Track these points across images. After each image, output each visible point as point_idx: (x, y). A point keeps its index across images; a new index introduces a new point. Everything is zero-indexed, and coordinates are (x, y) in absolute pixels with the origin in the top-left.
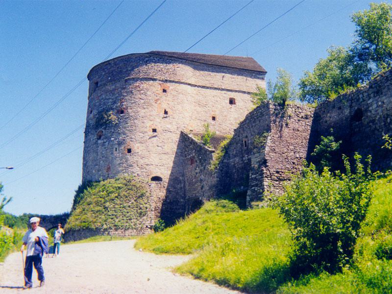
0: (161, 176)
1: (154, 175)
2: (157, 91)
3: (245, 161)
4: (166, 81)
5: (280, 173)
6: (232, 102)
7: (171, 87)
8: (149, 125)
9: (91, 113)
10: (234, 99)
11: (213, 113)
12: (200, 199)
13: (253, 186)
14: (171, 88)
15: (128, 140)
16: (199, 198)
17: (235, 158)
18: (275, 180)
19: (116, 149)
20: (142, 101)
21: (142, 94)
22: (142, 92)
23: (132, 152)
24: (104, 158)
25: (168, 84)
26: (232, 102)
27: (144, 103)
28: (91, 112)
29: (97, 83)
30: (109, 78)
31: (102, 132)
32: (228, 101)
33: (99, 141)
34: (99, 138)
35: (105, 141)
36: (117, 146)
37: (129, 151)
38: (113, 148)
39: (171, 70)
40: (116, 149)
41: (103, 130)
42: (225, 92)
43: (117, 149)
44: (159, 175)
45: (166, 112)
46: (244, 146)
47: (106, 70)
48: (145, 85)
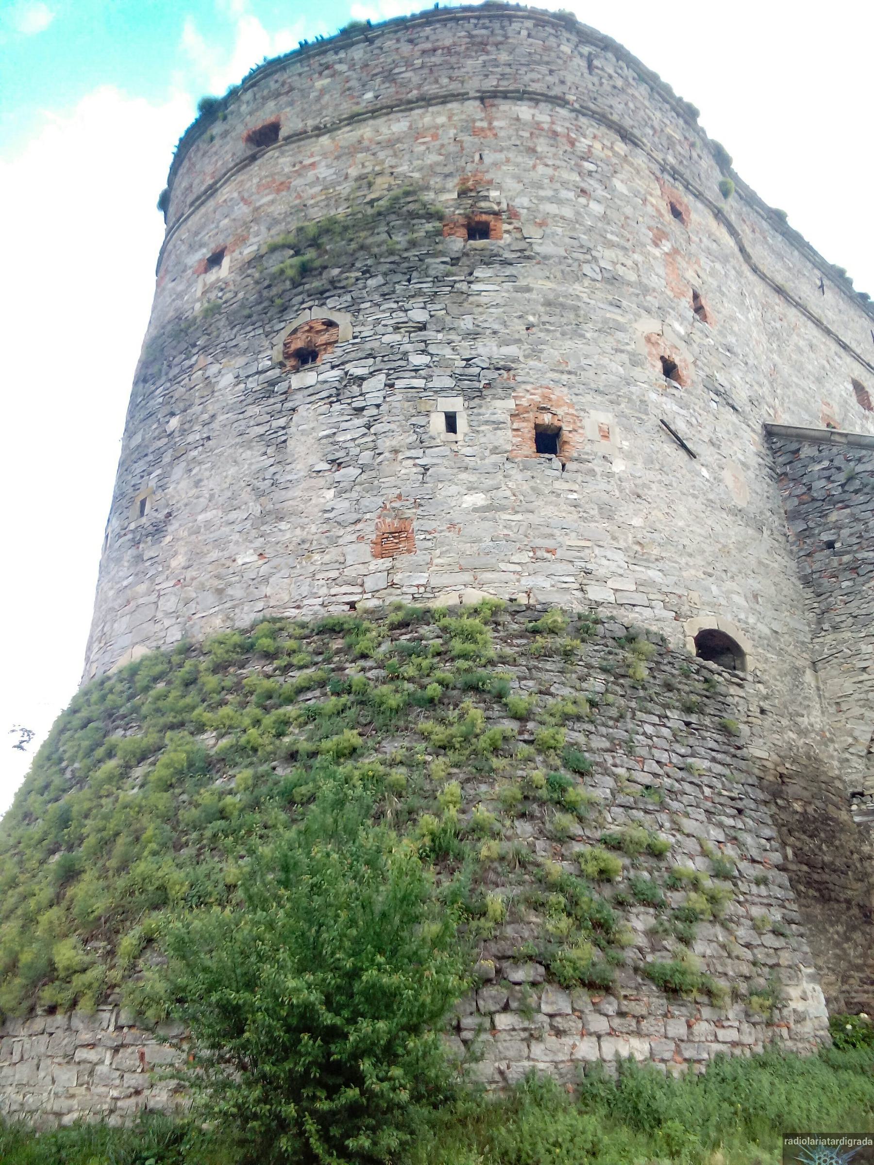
1: (709, 623)
15: (529, 370)
21: (590, 173)
24: (352, 472)
30: (369, 95)
31: (330, 324)
34: (306, 357)
35: (359, 372)
36: (456, 404)
37: (548, 441)
38: (428, 414)
41: (343, 320)
43: (461, 423)
47: (342, 67)
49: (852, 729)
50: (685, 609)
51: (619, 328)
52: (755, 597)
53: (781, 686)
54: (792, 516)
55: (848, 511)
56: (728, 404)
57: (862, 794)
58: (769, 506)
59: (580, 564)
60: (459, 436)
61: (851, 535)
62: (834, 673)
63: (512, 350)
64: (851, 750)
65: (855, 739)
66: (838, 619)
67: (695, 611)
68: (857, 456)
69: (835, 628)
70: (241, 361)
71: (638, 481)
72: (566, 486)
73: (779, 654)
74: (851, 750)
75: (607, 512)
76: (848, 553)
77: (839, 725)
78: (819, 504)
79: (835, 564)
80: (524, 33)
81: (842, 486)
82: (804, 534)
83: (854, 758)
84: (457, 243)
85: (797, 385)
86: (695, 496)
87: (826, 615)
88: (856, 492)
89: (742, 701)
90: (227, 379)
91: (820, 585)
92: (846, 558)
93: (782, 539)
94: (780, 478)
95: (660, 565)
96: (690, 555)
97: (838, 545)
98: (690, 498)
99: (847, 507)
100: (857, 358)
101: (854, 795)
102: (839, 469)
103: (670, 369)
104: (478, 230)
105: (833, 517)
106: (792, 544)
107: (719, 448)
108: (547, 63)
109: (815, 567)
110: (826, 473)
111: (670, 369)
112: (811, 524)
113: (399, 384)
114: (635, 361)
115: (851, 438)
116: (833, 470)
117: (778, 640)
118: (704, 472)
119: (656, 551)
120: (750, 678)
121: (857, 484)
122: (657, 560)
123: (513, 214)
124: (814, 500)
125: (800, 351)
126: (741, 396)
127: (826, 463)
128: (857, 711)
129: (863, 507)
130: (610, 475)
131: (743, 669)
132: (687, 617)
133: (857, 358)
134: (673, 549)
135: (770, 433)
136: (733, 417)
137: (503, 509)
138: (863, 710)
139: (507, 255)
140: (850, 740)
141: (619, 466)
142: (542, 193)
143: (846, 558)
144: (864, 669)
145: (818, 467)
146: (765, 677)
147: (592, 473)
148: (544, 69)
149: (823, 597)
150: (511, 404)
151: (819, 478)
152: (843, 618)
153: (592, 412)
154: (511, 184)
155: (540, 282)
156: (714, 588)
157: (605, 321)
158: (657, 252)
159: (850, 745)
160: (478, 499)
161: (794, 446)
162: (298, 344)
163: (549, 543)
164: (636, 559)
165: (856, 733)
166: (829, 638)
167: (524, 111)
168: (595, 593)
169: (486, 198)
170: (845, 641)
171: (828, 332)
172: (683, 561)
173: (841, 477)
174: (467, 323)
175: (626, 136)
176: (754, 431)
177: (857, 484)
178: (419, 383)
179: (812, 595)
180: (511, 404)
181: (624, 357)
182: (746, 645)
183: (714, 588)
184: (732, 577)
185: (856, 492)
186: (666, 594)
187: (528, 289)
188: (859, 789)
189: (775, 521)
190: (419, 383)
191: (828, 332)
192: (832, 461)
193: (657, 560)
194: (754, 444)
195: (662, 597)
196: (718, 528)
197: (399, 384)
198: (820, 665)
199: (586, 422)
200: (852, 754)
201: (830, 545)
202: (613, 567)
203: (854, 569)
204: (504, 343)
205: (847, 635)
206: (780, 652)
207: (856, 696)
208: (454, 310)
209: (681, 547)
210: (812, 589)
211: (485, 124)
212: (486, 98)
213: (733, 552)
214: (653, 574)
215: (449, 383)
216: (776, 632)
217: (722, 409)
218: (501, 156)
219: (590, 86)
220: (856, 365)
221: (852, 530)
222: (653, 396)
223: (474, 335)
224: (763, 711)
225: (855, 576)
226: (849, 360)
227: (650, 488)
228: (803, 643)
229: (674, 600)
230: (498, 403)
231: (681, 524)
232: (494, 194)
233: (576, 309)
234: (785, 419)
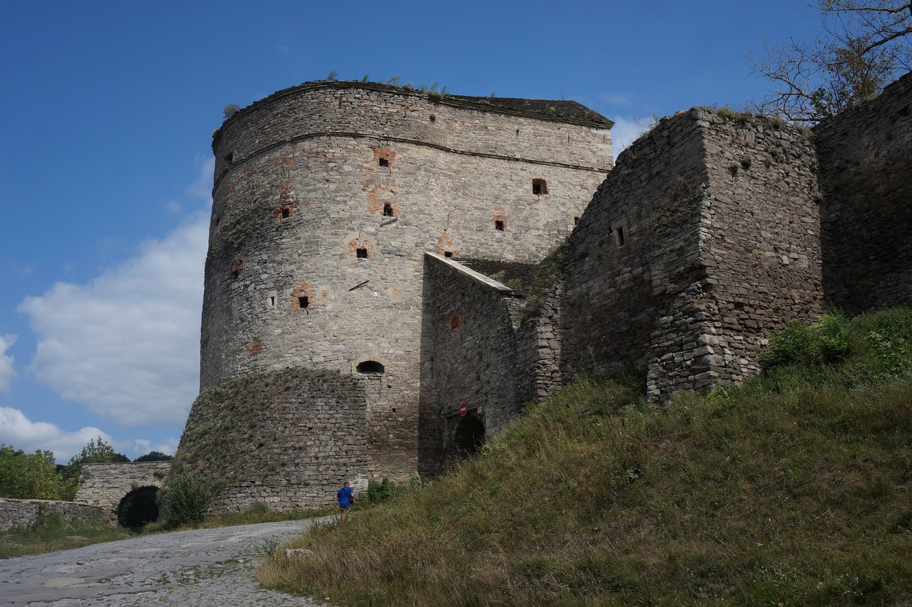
0: (383, 362)
1: (364, 358)
2: (367, 162)
3: (623, 287)
4: (387, 139)
5: (746, 308)
6: (539, 187)
7: (402, 154)
8: (350, 238)
9: (217, 225)
10: (543, 182)
11: (496, 213)
12: (479, 411)
13: (669, 349)
14: (398, 156)
16: (476, 410)
17: (591, 283)
18: (732, 329)
19: (273, 298)
20: (332, 186)
22: (331, 165)
23: (310, 306)
25: (393, 146)
26: (539, 187)
27: (337, 190)
28: (218, 221)
29: (229, 157)
31: (241, 261)
32: (529, 187)
33: (235, 285)
35: (248, 283)
36: (274, 293)
37: (304, 302)
39: (397, 117)
40: (273, 298)
42: (525, 165)
43: (276, 300)
44: (376, 357)
45: (388, 210)
46: (618, 243)
48: (337, 148)
51: (336, 244)
52: (397, 341)
59: (311, 349)
60: (275, 307)
63: (293, 267)
70: (221, 275)
72: (305, 321)
75: (322, 327)
80: (310, 97)
84: (279, 221)
90: (218, 283)
103: (362, 253)
104: (286, 213)
108: (319, 112)
111: (362, 253)
113: (258, 288)
114: (342, 257)
118: (376, 294)
119: (342, 338)
123: (297, 202)
130: (325, 312)
137: (287, 333)
139: (294, 224)
141: (329, 307)
142: (310, 188)
147: (318, 312)
148: (316, 117)
150: (291, 290)
153: (320, 287)
154: (298, 186)
155: (305, 234)
157: (330, 244)
158: (364, 194)
160: (279, 331)
162: (234, 270)
163: (301, 344)
164: (333, 342)
167: (306, 145)
168: (316, 359)
169: (288, 197)
174: (279, 258)
175: (355, 136)
178: (263, 286)
180: (291, 290)
181: (337, 257)
187: (299, 238)
190: (263, 286)
197: (258, 288)
199: (317, 292)
202: (324, 348)
204: (291, 264)
208: (275, 252)
211: (291, 156)
212: (294, 141)
214: (341, 347)
215: (272, 285)
218: (295, 173)
219: (339, 116)
222: (350, 270)
223: (280, 263)
224: (389, 387)
230: (288, 291)
231: (357, 322)
232: (292, 193)
233: (317, 242)
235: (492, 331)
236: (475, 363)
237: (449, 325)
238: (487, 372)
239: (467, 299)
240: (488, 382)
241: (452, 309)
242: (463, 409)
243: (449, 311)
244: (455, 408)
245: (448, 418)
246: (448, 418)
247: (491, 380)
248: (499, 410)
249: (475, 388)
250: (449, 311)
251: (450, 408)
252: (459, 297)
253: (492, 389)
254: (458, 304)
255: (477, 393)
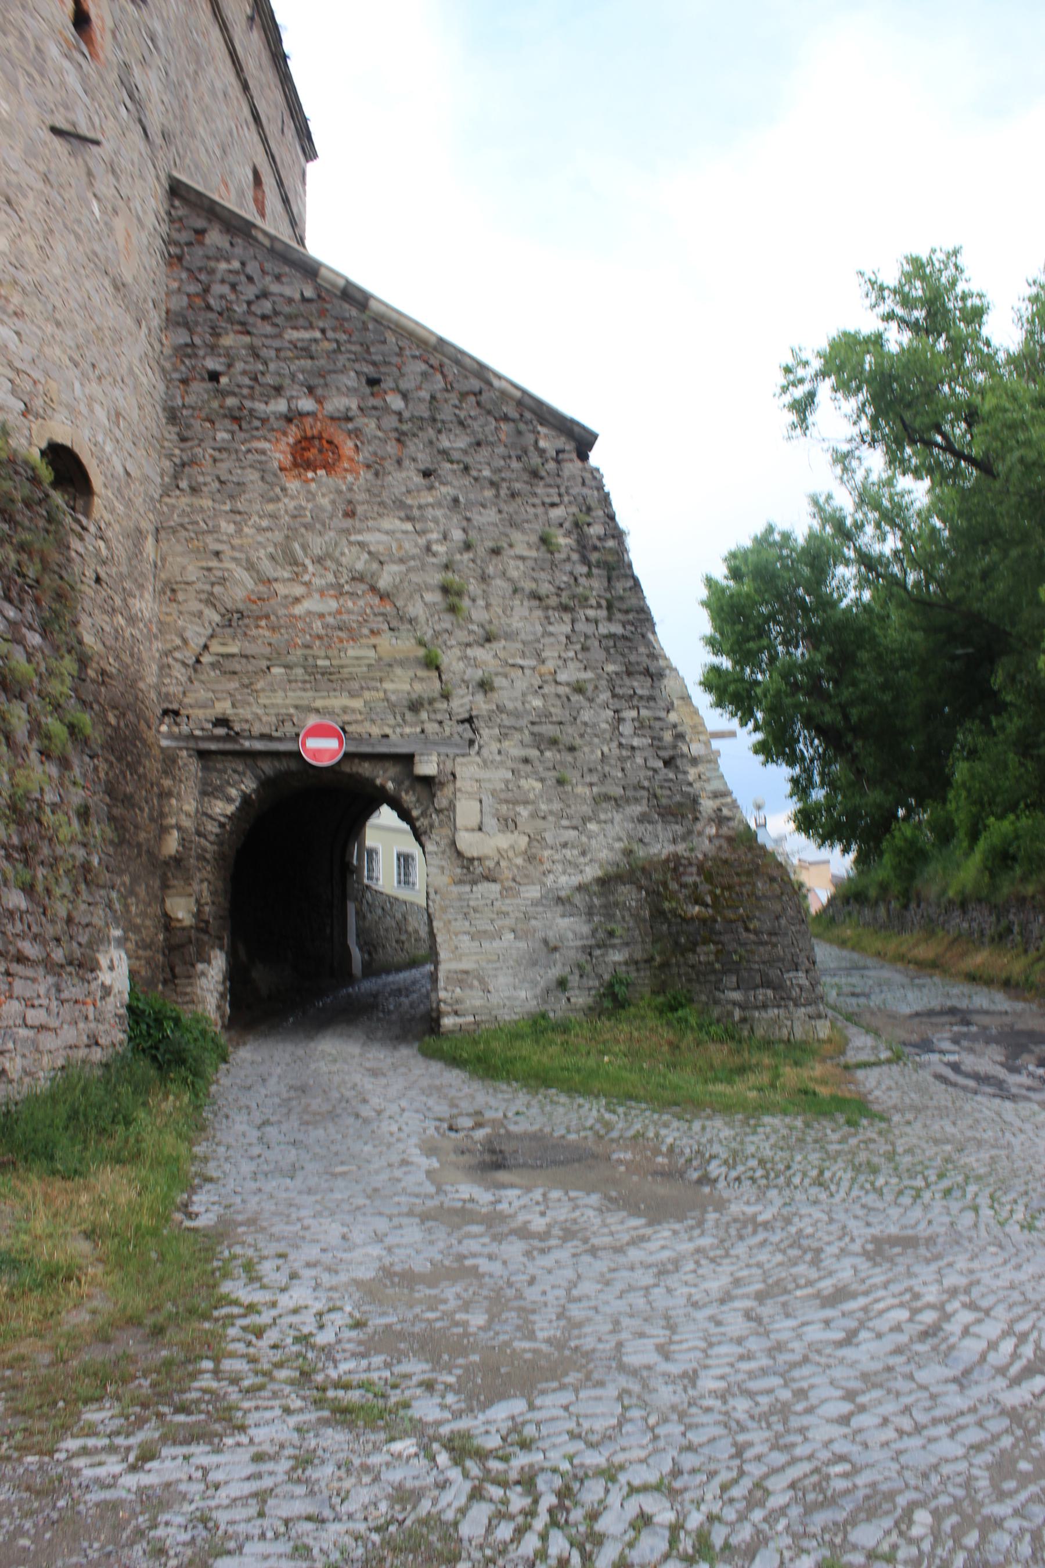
49: (184, 629)
50: (38, 403)
53: (120, 552)
54: (174, 320)
55: (247, 339)
56: (140, 121)
57: (176, 713)
58: (153, 294)
61: (244, 373)
62: (179, 548)
64: (177, 655)
65: (185, 641)
66: (201, 479)
67: (49, 412)
68: (277, 270)
69: (194, 490)
71: (13, 179)
73: (127, 506)
74: (177, 655)
76: (234, 394)
77: (168, 619)
78: (213, 316)
79: (215, 404)
81: (249, 303)
82: (185, 352)
83: (178, 666)
85: (203, 142)
86: (78, 238)
87: (187, 469)
88: (264, 317)
89: (77, 559)
91: (189, 427)
92: (231, 401)
93: (157, 346)
94: (175, 260)
95: (19, 324)
96: (58, 324)
97: (224, 380)
98: (72, 237)
99: (248, 333)
100: (265, 141)
101: (166, 712)
102: (250, 279)
105: (228, 340)
106: (166, 359)
107: (118, 179)
109: (190, 400)
110: (232, 278)
112: (197, 341)
115: (278, 246)
116: (243, 278)
117: (128, 485)
120: (92, 529)
121: (266, 306)
122: (16, 314)
124: (209, 307)
125: (213, 92)
126: (155, 120)
127: (236, 265)
128: (195, 606)
129: (268, 342)
131: (87, 514)
132: (37, 416)
133: (265, 141)
134: (39, 306)
135: (176, 190)
136: (142, 145)
138: (202, 606)
140: (178, 642)
143: (231, 401)
144: (217, 554)
145: (223, 266)
146: (109, 534)
149: (189, 444)
151: (223, 281)
152: (208, 479)
156: (77, 385)
159: (177, 648)
161: (200, 223)
165: (188, 634)
166: (185, 501)
170: (202, 510)
171: (245, 87)
172: (50, 328)
173: (250, 292)
176: (158, 178)
177: (266, 306)
179: (175, 437)
182: (97, 481)
183: (77, 385)
184: (99, 378)
185: (264, 317)
186: (18, 371)
188: (175, 706)
189: (155, 319)
191: (245, 87)
192: (243, 264)
193: (16, 314)
194: (155, 197)
195: (12, 375)
196: (96, 300)
198: (163, 535)
200: (176, 659)
201: (214, 377)
203: (237, 420)
205: (207, 503)
206: (129, 503)
207: (199, 586)
209: (50, 307)
210: (176, 429)
213: (107, 342)
216: (128, 474)
217: (132, 124)
220: (260, 148)
221: (248, 368)
224: (98, 580)
225: (236, 427)
226: (256, 138)
227: (25, 196)
228: (152, 499)
229: (28, 386)
231: (57, 271)
234: (184, 178)
235: (517, 536)
236: (416, 609)
237: (279, 453)
238: (477, 652)
239: (396, 402)
240: (485, 686)
241: (306, 404)
242: (332, 744)
243: (281, 406)
244: (257, 729)
245: (203, 755)
246: (203, 755)
247: (499, 682)
248: (532, 785)
249: (402, 684)
250: (281, 406)
251: (222, 721)
252: (350, 380)
253: (501, 709)
254: (337, 403)
255: (415, 706)
